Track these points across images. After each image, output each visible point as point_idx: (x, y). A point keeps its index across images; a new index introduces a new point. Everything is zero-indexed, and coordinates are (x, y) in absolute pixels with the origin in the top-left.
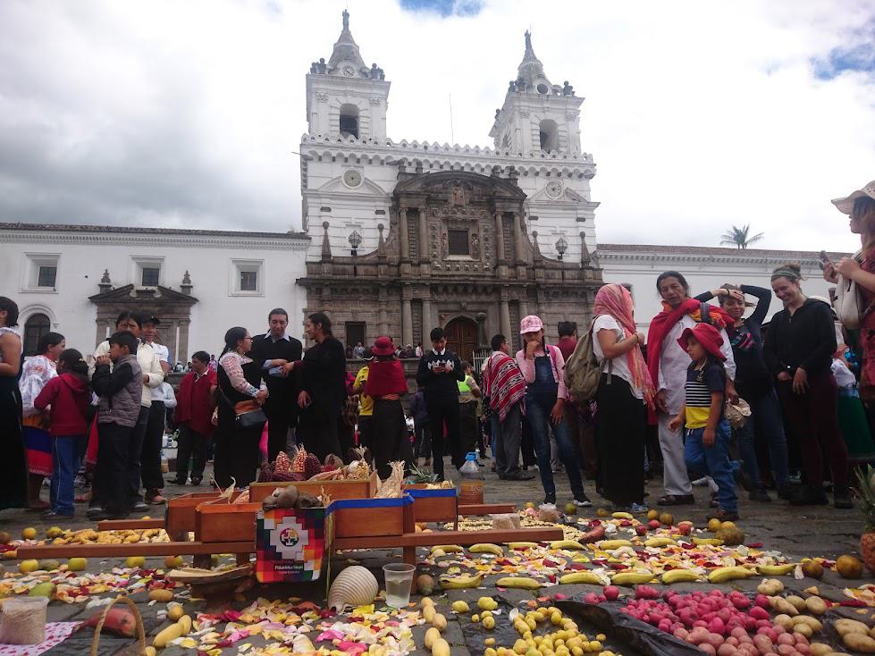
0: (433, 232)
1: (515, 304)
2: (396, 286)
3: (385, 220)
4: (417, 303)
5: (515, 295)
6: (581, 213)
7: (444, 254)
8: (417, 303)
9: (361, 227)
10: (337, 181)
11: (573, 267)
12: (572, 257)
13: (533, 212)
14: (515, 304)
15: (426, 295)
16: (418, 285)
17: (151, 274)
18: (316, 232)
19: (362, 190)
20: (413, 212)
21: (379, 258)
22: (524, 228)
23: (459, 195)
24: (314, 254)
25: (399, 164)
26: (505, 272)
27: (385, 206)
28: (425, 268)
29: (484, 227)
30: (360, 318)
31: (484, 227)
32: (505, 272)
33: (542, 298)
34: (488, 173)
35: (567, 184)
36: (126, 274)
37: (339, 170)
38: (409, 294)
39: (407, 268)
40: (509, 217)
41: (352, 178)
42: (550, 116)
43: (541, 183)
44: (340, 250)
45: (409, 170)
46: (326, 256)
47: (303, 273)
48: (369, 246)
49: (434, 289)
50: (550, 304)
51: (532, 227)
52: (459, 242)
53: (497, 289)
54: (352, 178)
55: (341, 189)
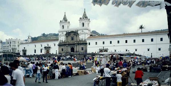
0: (70, 38)
1: (76, 46)
2: (65, 45)
3: (65, 38)
4: (67, 46)
8: (67, 46)
10: (61, 34)
12: (84, 40)
13: (80, 35)
14: (76, 46)
15: (68, 46)
19: (63, 35)
20: (67, 37)
21: (65, 42)
22: (79, 37)
26: (75, 42)
27: (65, 36)
29: (75, 37)
31: (75, 37)
32: (75, 42)
33: (80, 45)
34: (75, 31)
35: (84, 31)
36: (46, 46)
38: (66, 46)
40: (76, 36)
41: (63, 33)
42: (83, 22)
43: (81, 31)
45: (67, 32)
52: (72, 39)
54: (63, 33)
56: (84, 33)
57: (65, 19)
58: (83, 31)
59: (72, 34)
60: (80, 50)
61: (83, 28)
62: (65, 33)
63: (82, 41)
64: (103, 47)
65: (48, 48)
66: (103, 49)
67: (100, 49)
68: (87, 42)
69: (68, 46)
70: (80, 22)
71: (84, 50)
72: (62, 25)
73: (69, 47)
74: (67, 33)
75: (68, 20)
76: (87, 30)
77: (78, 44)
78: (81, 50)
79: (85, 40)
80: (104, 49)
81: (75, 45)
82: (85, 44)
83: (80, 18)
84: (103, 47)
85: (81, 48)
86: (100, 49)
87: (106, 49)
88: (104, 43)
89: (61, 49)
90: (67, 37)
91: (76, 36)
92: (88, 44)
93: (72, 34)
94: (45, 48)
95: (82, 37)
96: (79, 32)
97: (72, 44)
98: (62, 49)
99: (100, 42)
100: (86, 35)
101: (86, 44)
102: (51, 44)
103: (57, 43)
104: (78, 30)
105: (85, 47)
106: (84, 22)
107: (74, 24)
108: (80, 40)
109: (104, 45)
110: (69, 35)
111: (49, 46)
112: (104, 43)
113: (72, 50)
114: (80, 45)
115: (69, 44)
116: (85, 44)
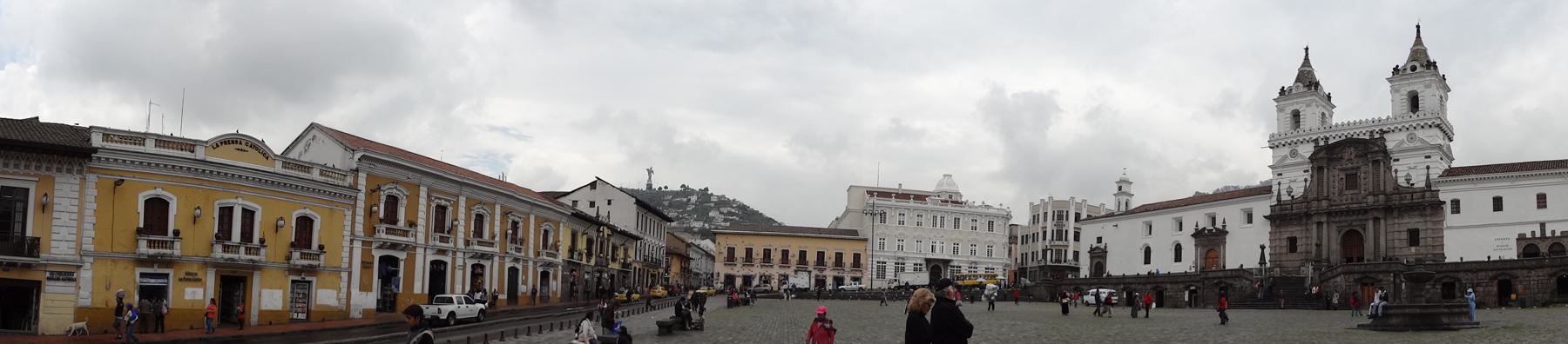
0: (1335, 177)
1: (1376, 220)
4: (1319, 224)
5: (1376, 214)
6: (1428, 152)
7: (1341, 192)
8: (1319, 224)
9: (1297, 182)
10: (1285, 157)
11: (1423, 191)
12: (1419, 182)
13: (1395, 156)
14: (1376, 220)
15: (1324, 219)
16: (1318, 213)
17: (1214, 220)
18: (1275, 189)
19: (1299, 160)
20: (1320, 169)
22: (1390, 168)
23: (1350, 153)
24: (1274, 201)
25: (1316, 141)
26: (1370, 199)
27: (1308, 166)
28: (1324, 204)
29: (1366, 175)
30: (1297, 234)
35: (1420, 133)
36: (1204, 223)
37: (1286, 151)
38: (1316, 219)
39: (1315, 204)
40: (1376, 162)
41: (1294, 154)
43: (1403, 136)
44: (1285, 197)
45: (1322, 143)
46: (1279, 200)
47: (1268, 213)
48: (1298, 191)
49: (1329, 214)
50: (1400, 216)
51: (1395, 165)
52: (1352, 180)
53: (1366, 211)
54: (1294, 154)
55: (1290, 161)
56: (1418, 144)
57: (1307, 80)
58: (1412, 138)
59: (1346, 156)
60: (1397, 243)
61: (1414, 116)
62: (1307, 150)
63: (1411, 189)
64: (1543, 225)
65: (1211, 239)
66: (1538, 235)
67: (1521, 238)
68: (1442, 197)
69: (1324, 219)
70: (1394, 91)
71: (1422, 242)
72: (1289, 110)
73: (1334, 227)
74: (1318, 150)
75: (1326, 87)
76: (1437, 131)
77: (1388, 210)
78: (1405, 244)
79: (1428, 184)
80: (1548, 234)
81: (1370, 215)
82: (1429, 211)
83: (1396, 70)
84: (1543, 225)
85: (1405, 236)
86: (1521, 238)
87: (1558, 234)
88: (1542, 201)
89: (1284, 243)
90: (1320, 169)
91: (1376, 162)
92: (1448, 208)
93: (1350, 153)
94: (1198, 234)
95: (1410, 170)
96: (1391, 144)
97: (1349, 212)
98: (1293, 242)
99: (1519, 197)
100: (1436, 158)
101: (1438, 206)
102: (1229, 214)
103: (1262, 208)
104: (1383, 132)
105: (1430, 225)
106: (1418, 87)
107: (1360, 100)
108: (1397, 187)
109: (1542, 215)
110: (1330, 160)
111: (1219, 225)
112: (1542, 201)
113: (1352, 240)
114: (1396, 213)
115: (1329, 214)
116: (1429, 211)
